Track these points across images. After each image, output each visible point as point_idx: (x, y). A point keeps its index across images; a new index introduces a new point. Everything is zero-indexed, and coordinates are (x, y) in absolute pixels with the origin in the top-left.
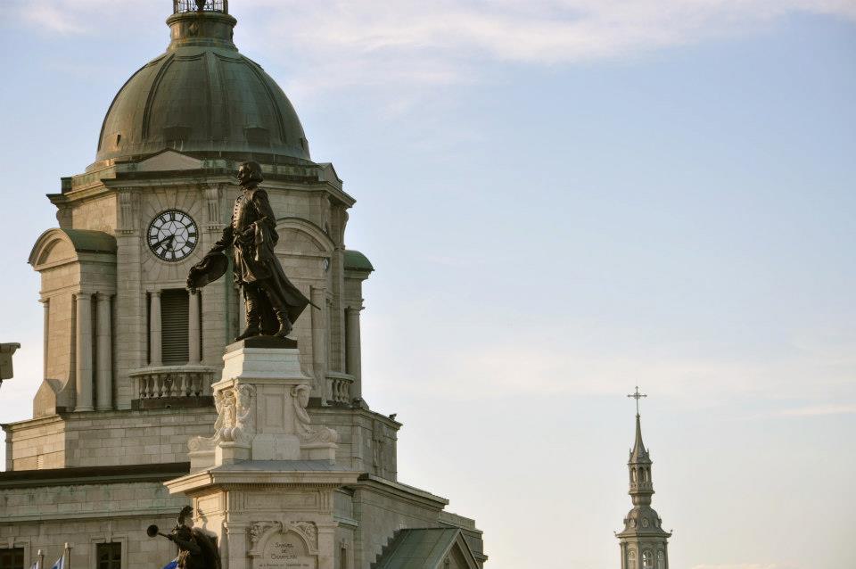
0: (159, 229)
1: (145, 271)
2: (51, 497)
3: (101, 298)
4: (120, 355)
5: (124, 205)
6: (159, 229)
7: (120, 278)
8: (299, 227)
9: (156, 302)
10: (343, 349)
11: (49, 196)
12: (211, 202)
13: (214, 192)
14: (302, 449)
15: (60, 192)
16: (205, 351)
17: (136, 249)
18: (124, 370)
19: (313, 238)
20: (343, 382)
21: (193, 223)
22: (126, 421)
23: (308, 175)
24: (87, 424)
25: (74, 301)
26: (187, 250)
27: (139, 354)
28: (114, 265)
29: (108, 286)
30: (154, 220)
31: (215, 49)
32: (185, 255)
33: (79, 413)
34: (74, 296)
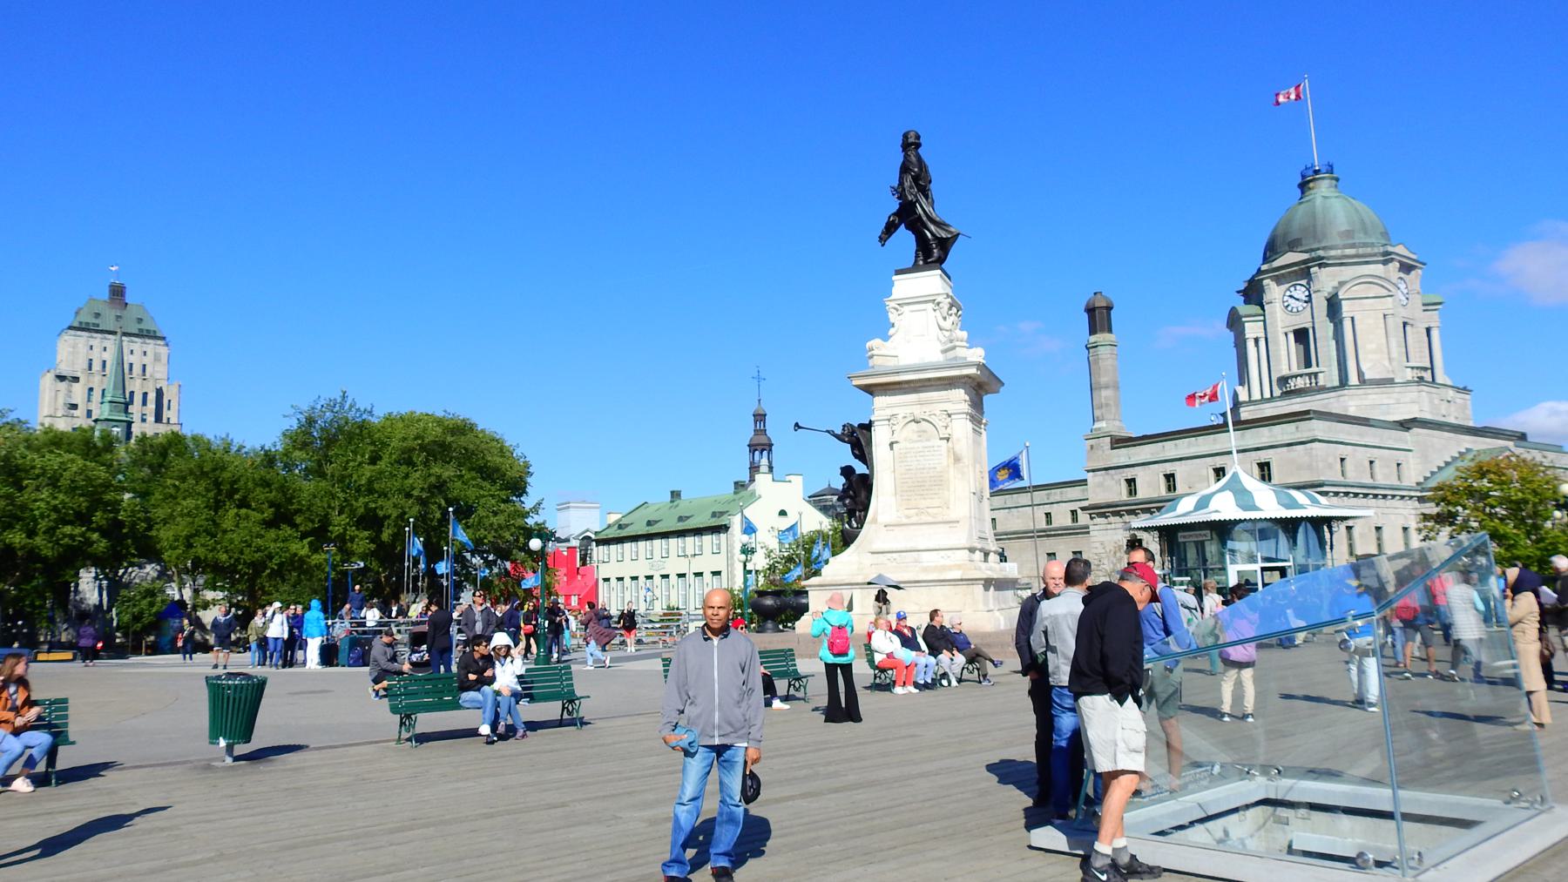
2: (1185, 444)
9: (1291, 336)
28: (1264, 321)
32: (1304, 308)
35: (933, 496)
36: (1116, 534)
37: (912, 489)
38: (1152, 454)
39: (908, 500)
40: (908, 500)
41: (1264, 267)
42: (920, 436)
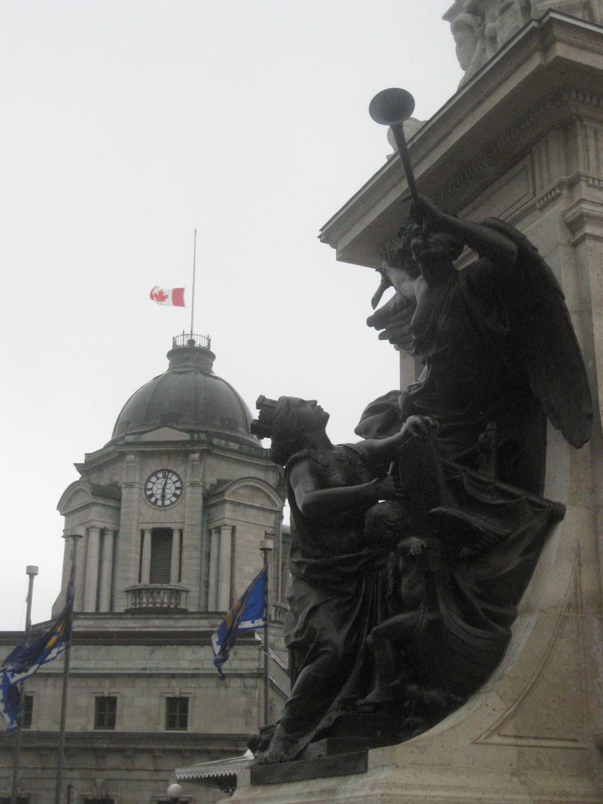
0: (154, 483)
3: (107, 532)
5: (129, 464)
6: (154, 483)
7: (122, 518)
8: (258, 486)
9: (148, 538)
11: (76, 465)
12: (194, 463)
13: (197, 456)
16: (184, 575)
17: (136, 497)
18: (121, 586)
19: (269, 496)
20: (283, 611)
21: (180, 480)
26: (173, 499)
27: (134, 575)
29: (113, 524)
30: (151, 477)
32: (172, 503)
33: (87, 613)
41: (130, 439)
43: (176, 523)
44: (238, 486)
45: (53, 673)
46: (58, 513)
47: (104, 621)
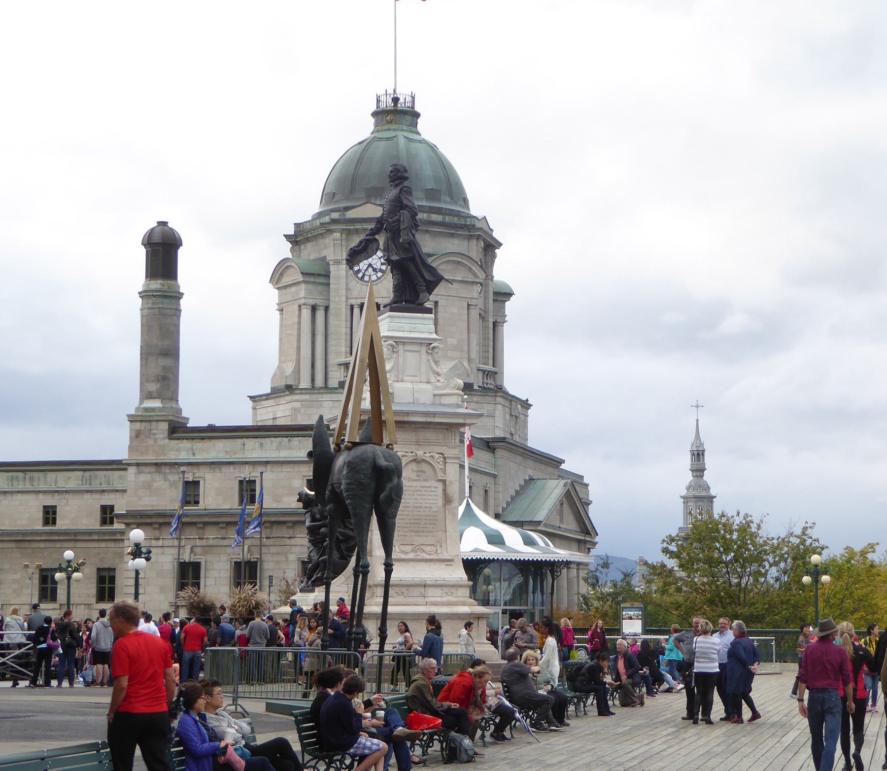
1: (349, 289)
2: (275, 445)
4: (331, 349)
5: (335, 242)
7: (332, 294)
10: (491, 350)
11: (285, 236)
14: (435, 395)
15: (293, 234)
17: (343, 273)
18: (334, 360)
19: (471, 268)
22: (334, 396)
23: (468, 223)
24: (307, 397)
25: (300, 310)
27: (343, 348)
28: (328, 285)
31: (405, 134)
32: (378, 278)
33: (301, 389)
34: (300, 306)
35: (427, 534)
36: (163, 554)
37: (408, 525)
38: (226, 452)
39: (404, 536)
40: (404, 536)
42: (419, 476)
43: (383, 297)
44: (439, 262)
45: (272, 461)
46: (271, 285)
47: (316, 396)
